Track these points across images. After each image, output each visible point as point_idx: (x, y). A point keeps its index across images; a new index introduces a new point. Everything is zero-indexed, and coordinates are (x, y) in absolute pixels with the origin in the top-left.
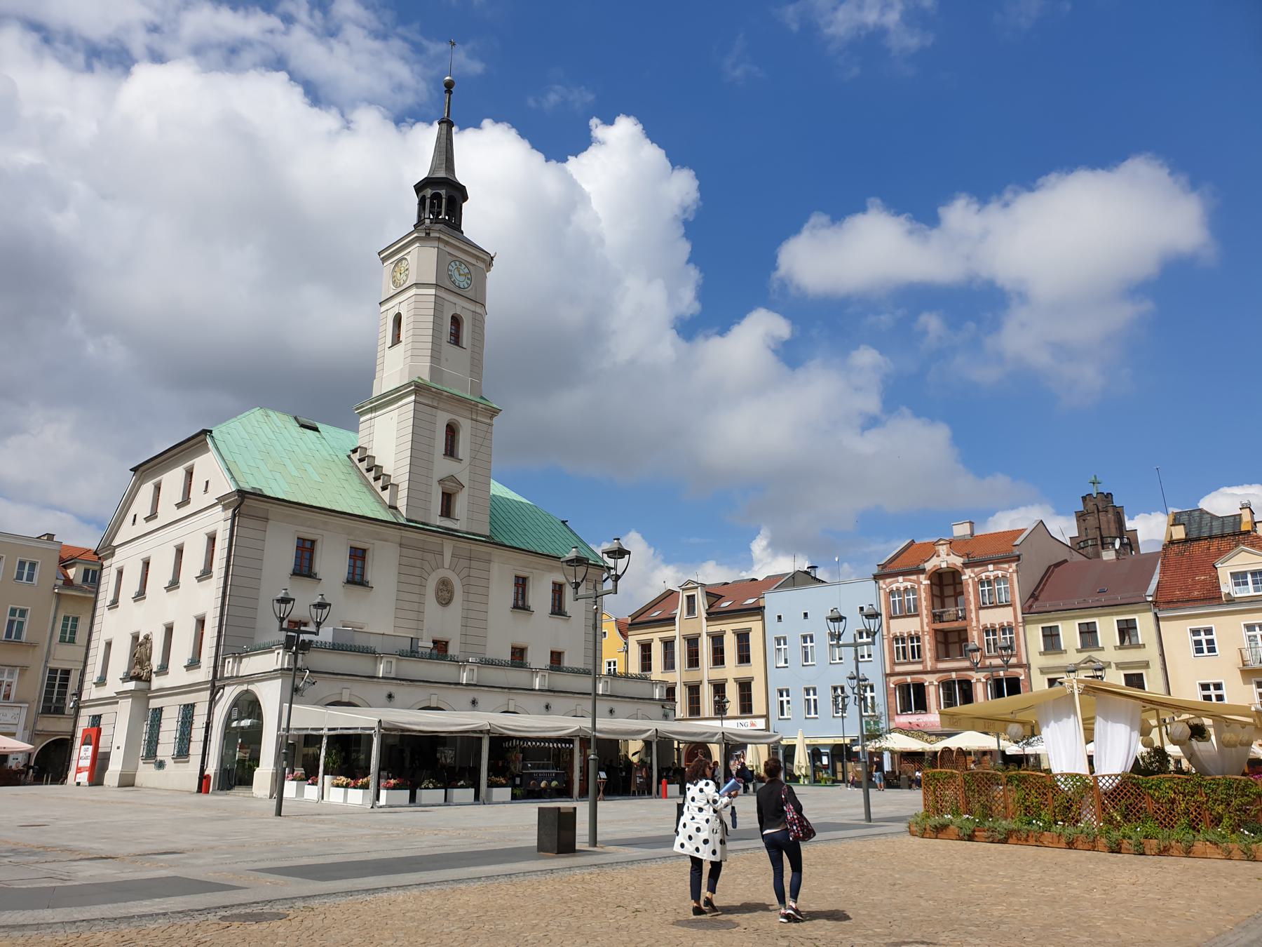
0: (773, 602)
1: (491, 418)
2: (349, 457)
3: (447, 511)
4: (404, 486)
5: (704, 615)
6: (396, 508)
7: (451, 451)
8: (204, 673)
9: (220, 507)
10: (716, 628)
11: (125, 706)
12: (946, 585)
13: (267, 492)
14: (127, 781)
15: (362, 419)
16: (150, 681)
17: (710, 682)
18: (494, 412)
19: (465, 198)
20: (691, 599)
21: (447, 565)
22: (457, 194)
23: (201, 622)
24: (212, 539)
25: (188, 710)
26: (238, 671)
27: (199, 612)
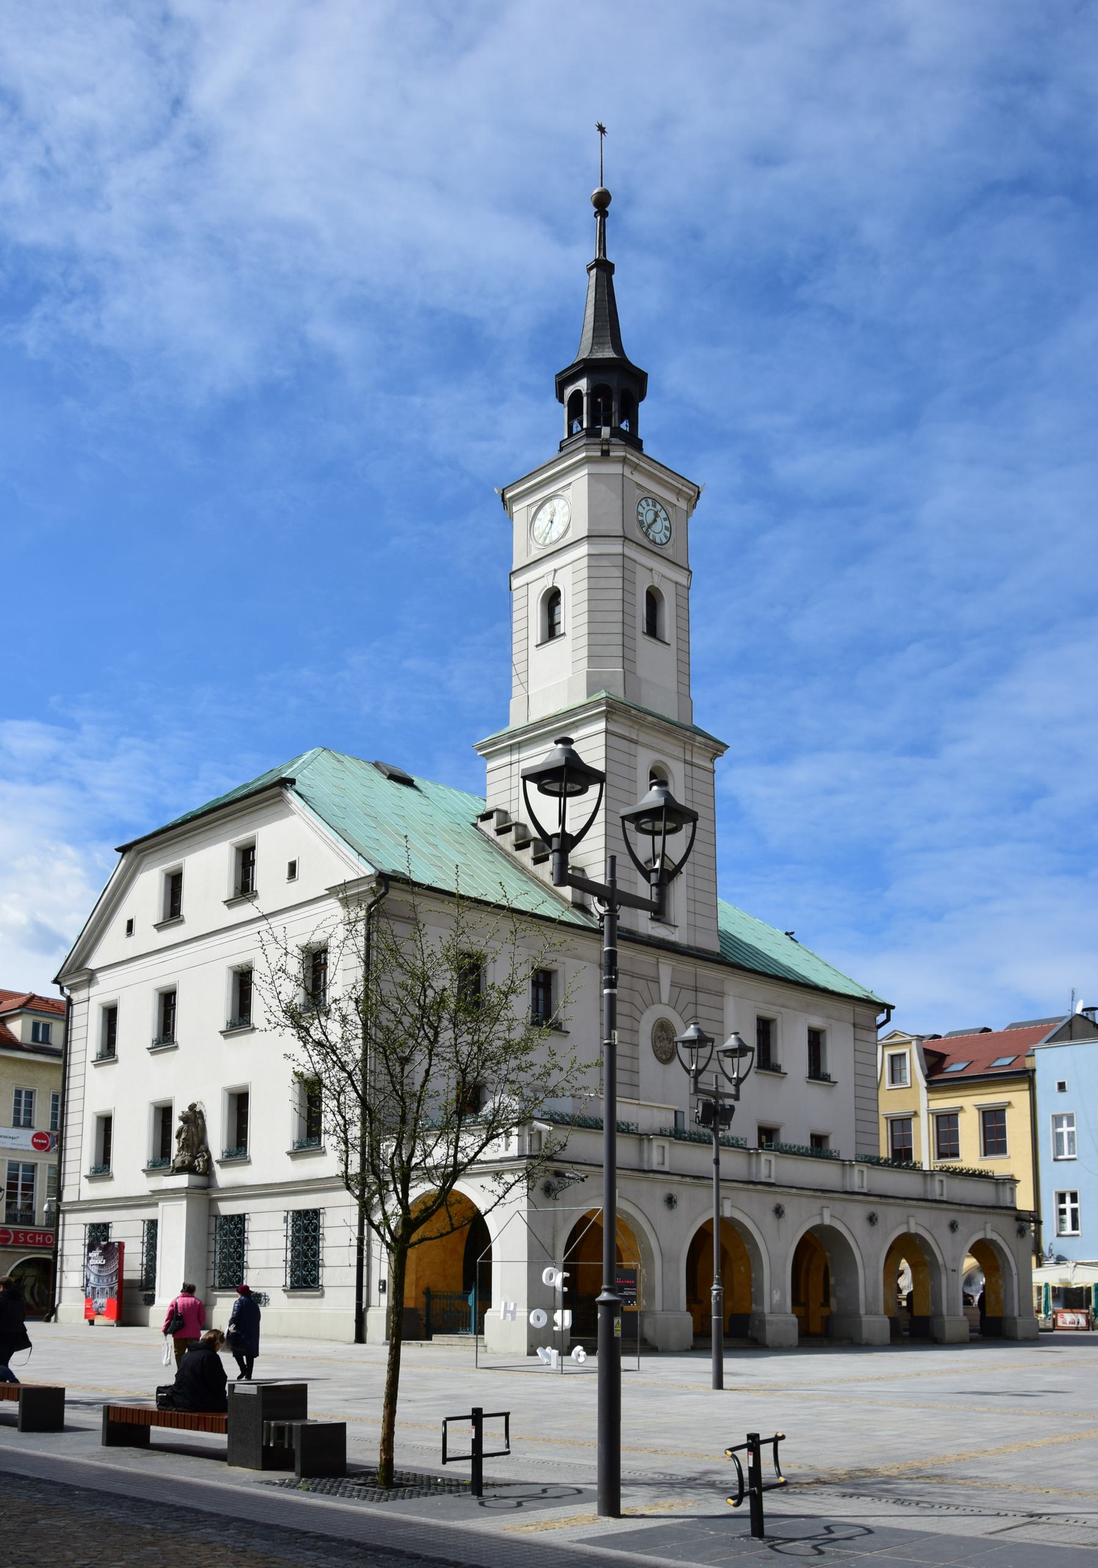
0: (1050, 1062)
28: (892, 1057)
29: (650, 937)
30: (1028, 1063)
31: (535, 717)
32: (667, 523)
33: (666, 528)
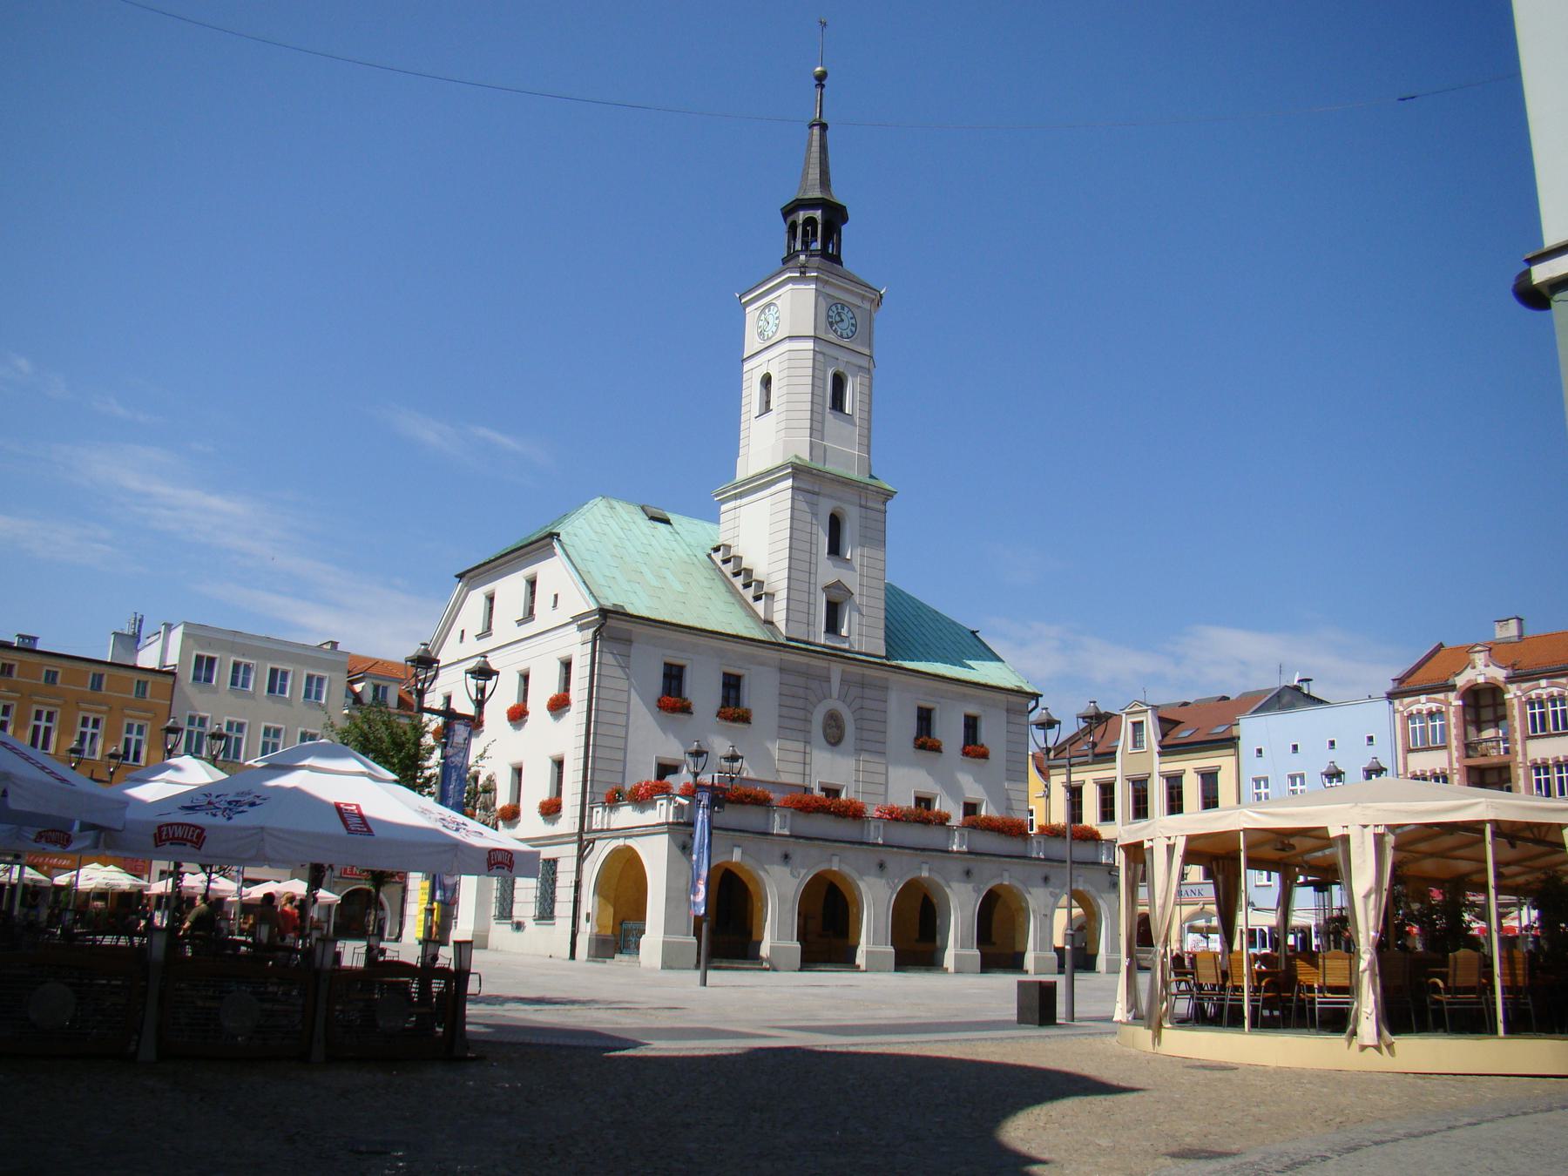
0: (1251, 729)
1: (884, 503)
2: (709, 556)
3: (833, 626)
4: (782, 595)
5: (1156, 748)
6: (772, 623)
7: (835, 549)
8: (568, 822)
9: (574, 626)
10: (1173, 765)
12: (1483, 705)
13: (631, 610)
15: (724, 508)
18: (888, 495)
19: (845, 219)
20: (1137, 726)
21: (835, 694)
22: (835, 216)
23: (559, 764)
24: (567, 665)
28: (1134, 724)
30: (1235, 734)
31: (751, 473)
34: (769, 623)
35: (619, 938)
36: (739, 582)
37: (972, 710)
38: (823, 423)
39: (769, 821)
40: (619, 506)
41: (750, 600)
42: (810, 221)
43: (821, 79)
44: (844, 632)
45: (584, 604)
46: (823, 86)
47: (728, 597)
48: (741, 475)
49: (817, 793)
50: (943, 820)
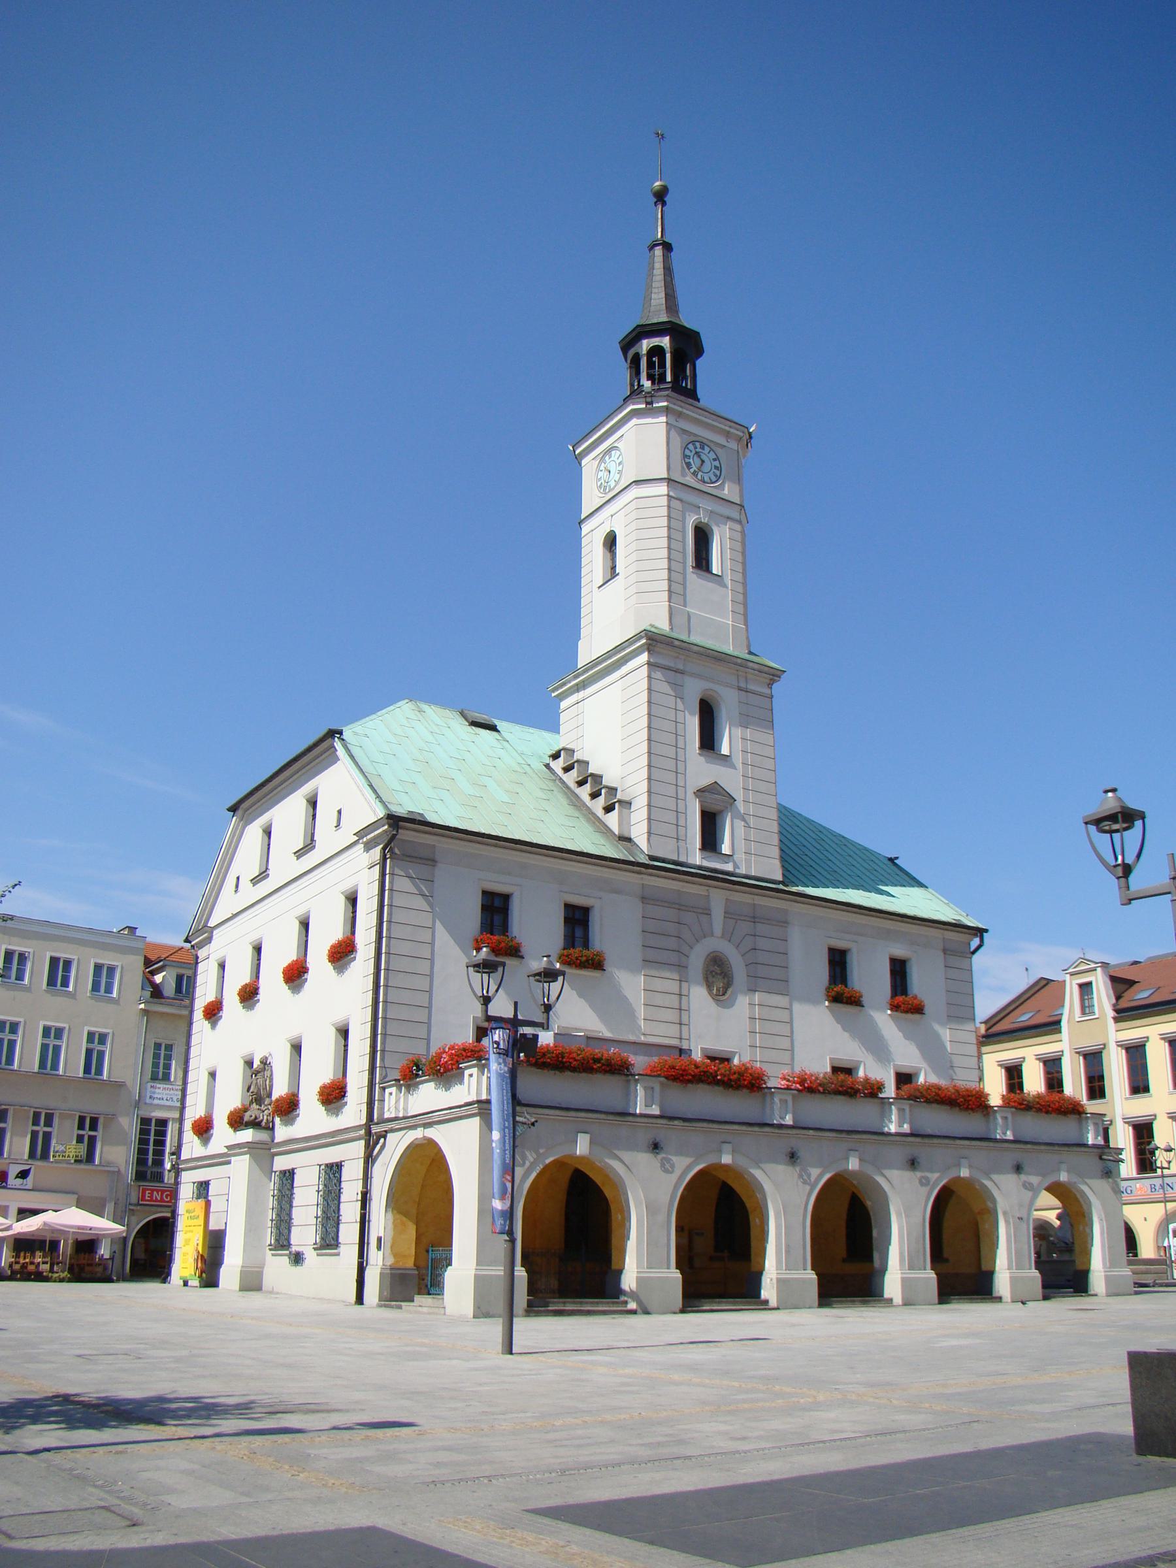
1: (770, 685)
2: (547, 766)
3: (710, 841)
4: (640, 803)
5: (1111, 1013)
6: (629, 840)
7: (708, 741)
8: (353, 1112)
10: (1133, 1032)
11: (242, 1164)
14: (252, 1283)
15: (564, 704)
16: (273, 1129)
17: (1126, 1121)
18: (774, 676)
19: (700, 352)
20: (1085, 988)
22: (688, 345)
23: (344, 1032)
24: (352, 900)
25: (334, 1171)
26: (405, 1109)
27: (339, 1017)
28: (1081, 986)
29: (700, 868)
32: (717, 463)
33: (716, 468)
34: (626, 839)
35: (419, 1276)
36: (584, 792)
37: (900, 952)
38: (684, 585)
39: (629, 1095)
40: (431, 711)
41: (600, 812)
42: (657, 351)
43: (661, 196)
44: (726, 848)
45: (369, 812)
46: (664, 204)
47: (571, 811)
48: (583, 660)
49: (697, 1056)
50: (873, 1090)
